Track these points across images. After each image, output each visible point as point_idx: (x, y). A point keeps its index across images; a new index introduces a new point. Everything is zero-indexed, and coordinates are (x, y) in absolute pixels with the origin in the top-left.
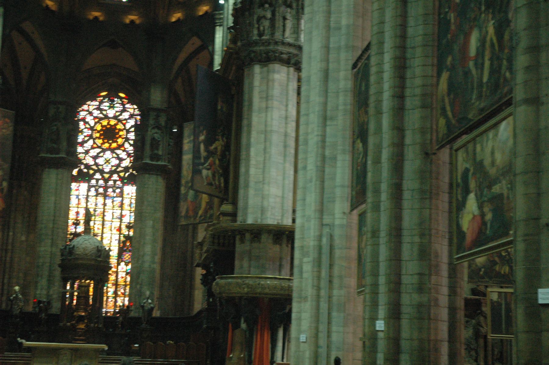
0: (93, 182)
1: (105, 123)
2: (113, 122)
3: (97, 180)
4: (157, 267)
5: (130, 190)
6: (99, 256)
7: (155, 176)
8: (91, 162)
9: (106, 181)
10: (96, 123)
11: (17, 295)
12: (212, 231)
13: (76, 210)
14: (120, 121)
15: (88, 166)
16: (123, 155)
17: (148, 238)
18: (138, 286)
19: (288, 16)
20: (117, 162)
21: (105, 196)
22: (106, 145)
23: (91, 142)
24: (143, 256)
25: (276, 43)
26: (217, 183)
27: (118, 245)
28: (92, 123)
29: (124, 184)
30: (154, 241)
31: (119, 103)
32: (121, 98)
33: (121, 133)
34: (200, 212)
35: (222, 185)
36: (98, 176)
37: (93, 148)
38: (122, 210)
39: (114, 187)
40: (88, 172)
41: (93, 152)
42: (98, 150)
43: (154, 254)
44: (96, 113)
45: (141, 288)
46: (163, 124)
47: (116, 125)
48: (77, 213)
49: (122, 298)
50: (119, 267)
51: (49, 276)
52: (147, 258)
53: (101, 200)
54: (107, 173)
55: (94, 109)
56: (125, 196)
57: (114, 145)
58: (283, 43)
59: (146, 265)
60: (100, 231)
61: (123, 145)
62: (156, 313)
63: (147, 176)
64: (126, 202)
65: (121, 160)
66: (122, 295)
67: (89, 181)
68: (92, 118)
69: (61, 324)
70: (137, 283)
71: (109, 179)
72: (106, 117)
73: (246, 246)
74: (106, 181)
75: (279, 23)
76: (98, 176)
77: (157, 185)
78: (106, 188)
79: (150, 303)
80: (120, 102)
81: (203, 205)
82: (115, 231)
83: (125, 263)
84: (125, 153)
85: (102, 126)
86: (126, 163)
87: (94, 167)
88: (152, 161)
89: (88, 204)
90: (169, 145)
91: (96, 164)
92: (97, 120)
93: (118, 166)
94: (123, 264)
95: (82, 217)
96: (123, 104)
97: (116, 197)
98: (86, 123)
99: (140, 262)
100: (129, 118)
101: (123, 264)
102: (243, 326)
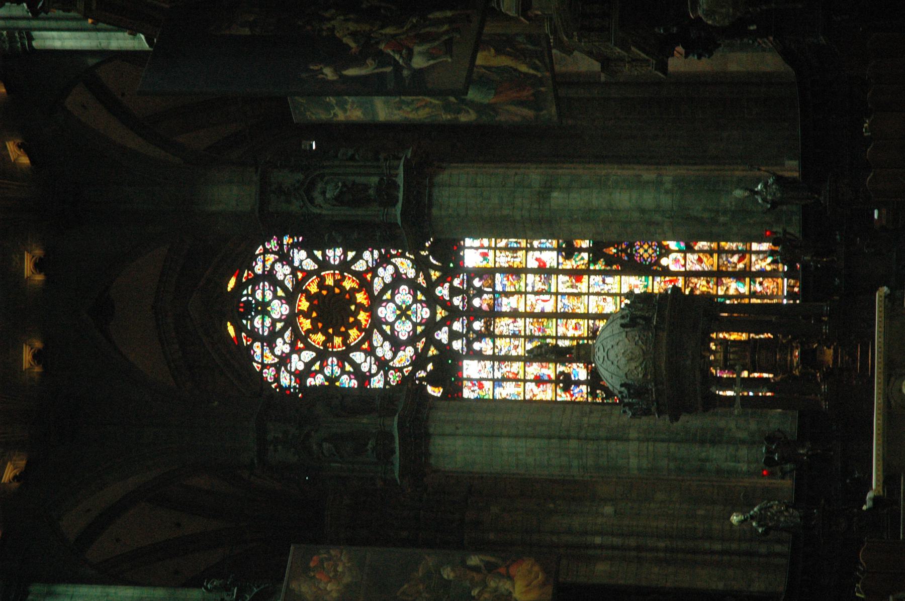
0: (457, 345)
1: (306, 324)
2: (304, 305)
3: (453, 335)
4: (670, 174)
5: (473, 254)
6: (648, 320)
7: (436, 191)
8: (406, 355)
9: (454, 313)
10: (309, 347)
11: (752, 518)
12: (570, 37)
13: (531, 386)
14: (299, 286)
15: (419, 361)
16: (386, 274)
17: (595, 202)
18: (722, 219)
20: (404, 289)
21: (492, 314)
22: (362, 316)
23: (358, 357)
24: (643, 211)
26: (446, 27)
27: (617, 278)
28: (308, 355)
29: (460, 268)
30: (602, 184)
31: (254, 291)
32: (240, 286)
33: (330, 282)
34: (524, 68)
35: (449, 14)
36: (442, 335)
37: (371, 351)
38: (526, 271)
39: (467, 293)
40: (433, 359)
41: (384, 350)
42: (377, 338)
43: (639, 184)
44: (282, 347)
45: (725, 212)
46: (301, 176)
47: (309, 297)
48: (539, 381)
49: (754, 258)
50: (673, 268)
51: (702, 442)
52: (648, 199)
53: (503, 325)
54: (433, 314)
55: (272, 351)
56: (491, 265)
57: (361, 297)
59: (666, 201)
60: (583, 323)
61: (359, 275)
62: (791, 168)
63: (435, 211)
64: (503, 260)
65: (398, 279)
66: (746, 260)
67: (457, 357)
68: (295, 357)
69: (825, 405)
70: (714, 221)
71: (447, 305)
72: (290, 321)
74: (454, 313)
76: (442, 335)
77: (458, 187)
78: (473, 314)
79: (766, 185)
80: (250, 287)
81: (504, 61)
82: (583, 287)
83: (660, 256)
84: (381, 270)
85: (314, 330)
86: (406, 267)
87: (420, 346)
88: (397, 201)
89: (514, 353)
90: (352, 158)
91: (413, 340)
92: (300, 345)
93: (413, 286)
94: (664, 261)
95: (550, 371)
96: (256, 280)
97: (493, 286)
98: (308, 371)
99: (658, 218)
100: (290, 262)
101: (664, 261)
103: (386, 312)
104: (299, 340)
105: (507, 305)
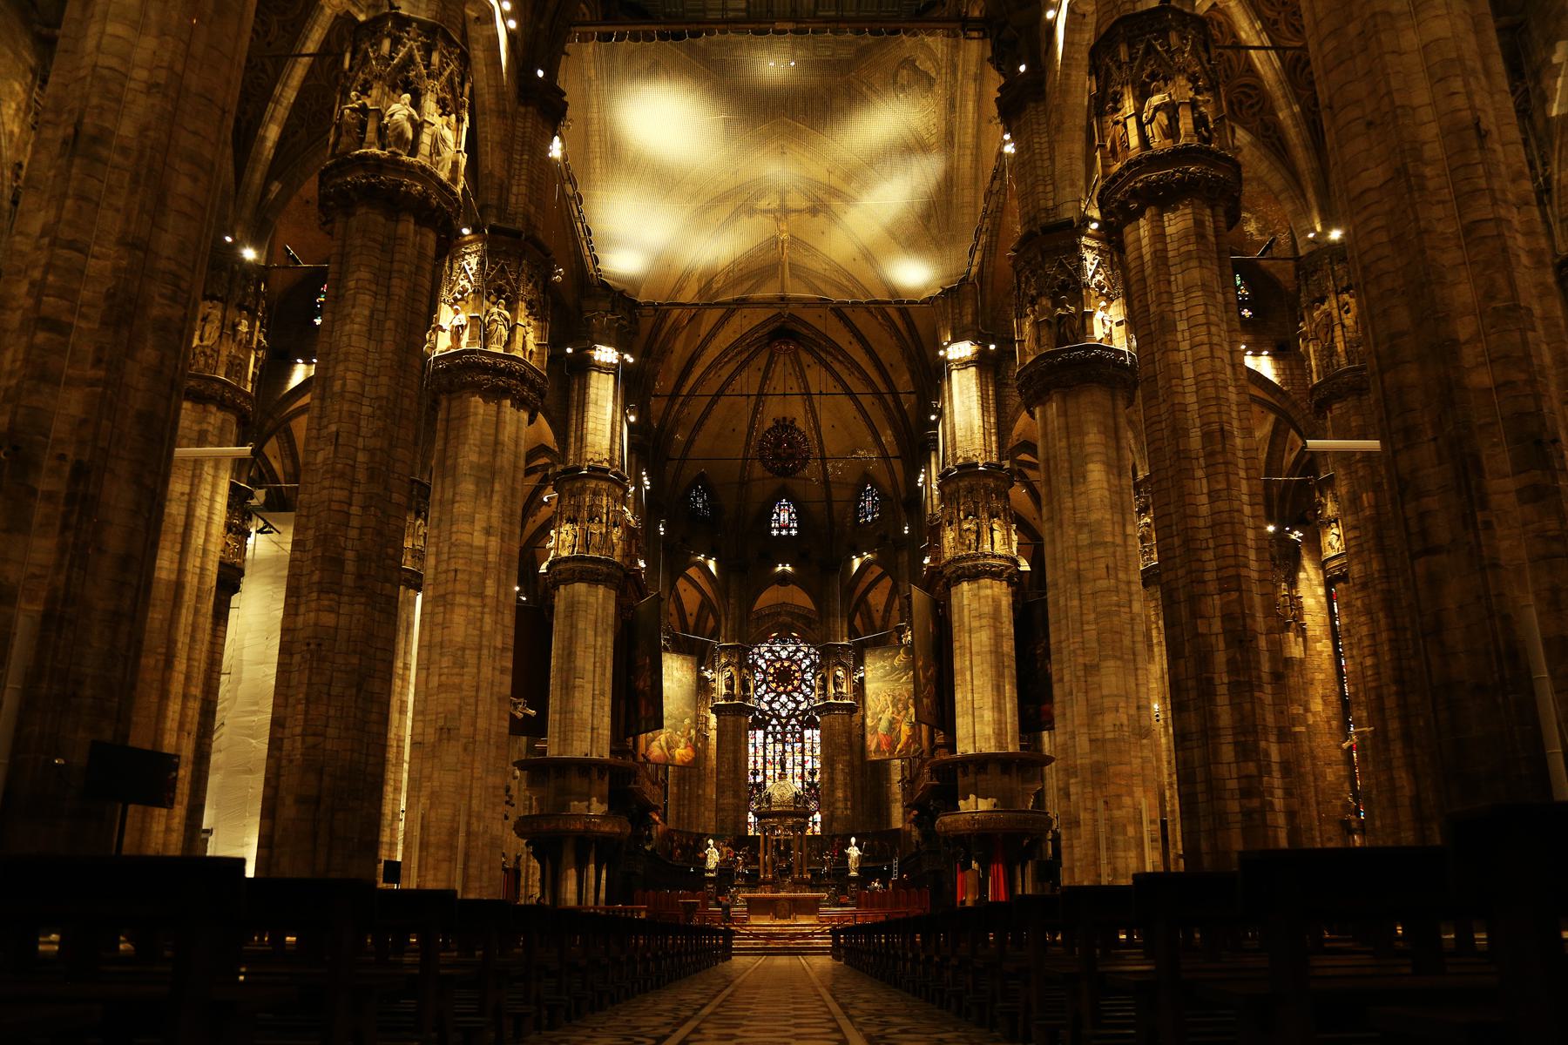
9: (784, 726)
15: (763, 712)
16: (800, 698)
19: (995, 526)
21: (784, 742)
25: (985, 556)
36: (774, 722)
41: (767, 698)
44: (767, 655)
52: (840, 805)
53: (779, 747)
58: (994, 557)
64: (808, 746)
67: (765, 729)
72: (779, 659)
73: (971, 779)
74: (784, 726)
75: (986, 536)
76: (774, 722)
78: (784, 734)
86: (803, 706)
91: (772, 709)
93: (796, 709)
95: (760, 767)
102: (975, 865)
103: (784, 698)
104: (771, 663)
105: (788, 748)
